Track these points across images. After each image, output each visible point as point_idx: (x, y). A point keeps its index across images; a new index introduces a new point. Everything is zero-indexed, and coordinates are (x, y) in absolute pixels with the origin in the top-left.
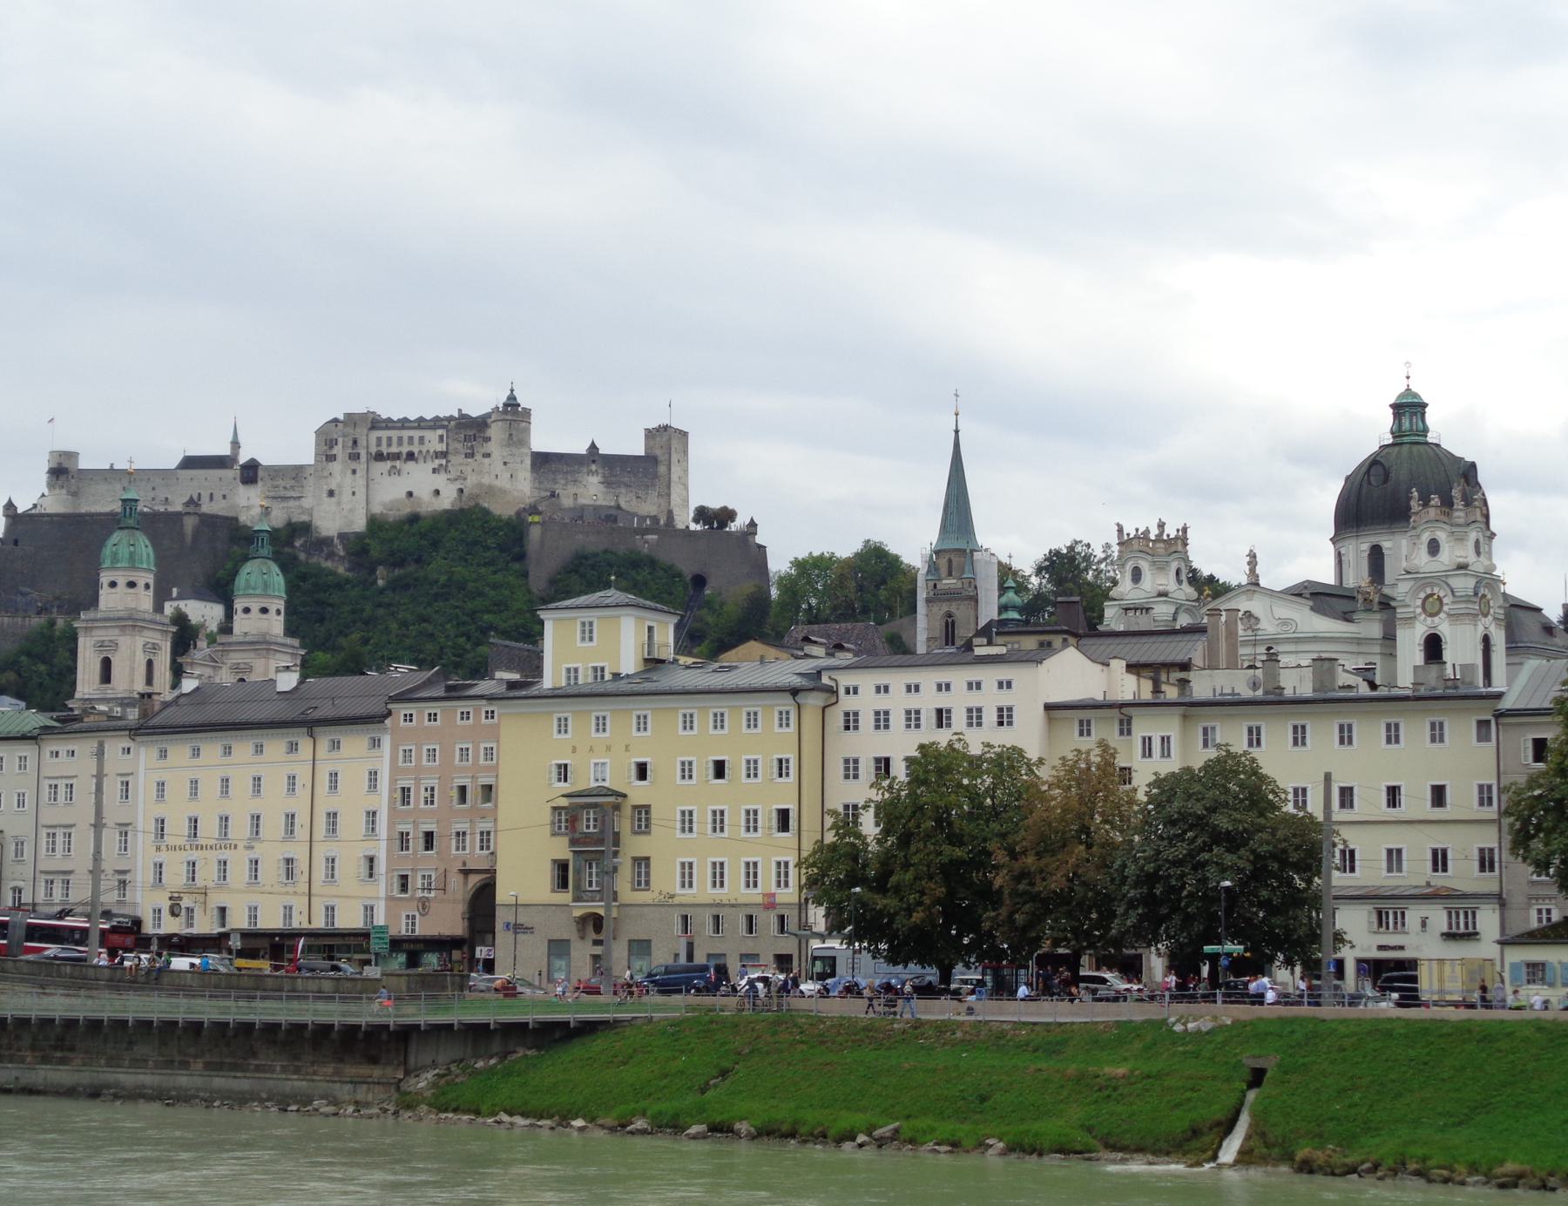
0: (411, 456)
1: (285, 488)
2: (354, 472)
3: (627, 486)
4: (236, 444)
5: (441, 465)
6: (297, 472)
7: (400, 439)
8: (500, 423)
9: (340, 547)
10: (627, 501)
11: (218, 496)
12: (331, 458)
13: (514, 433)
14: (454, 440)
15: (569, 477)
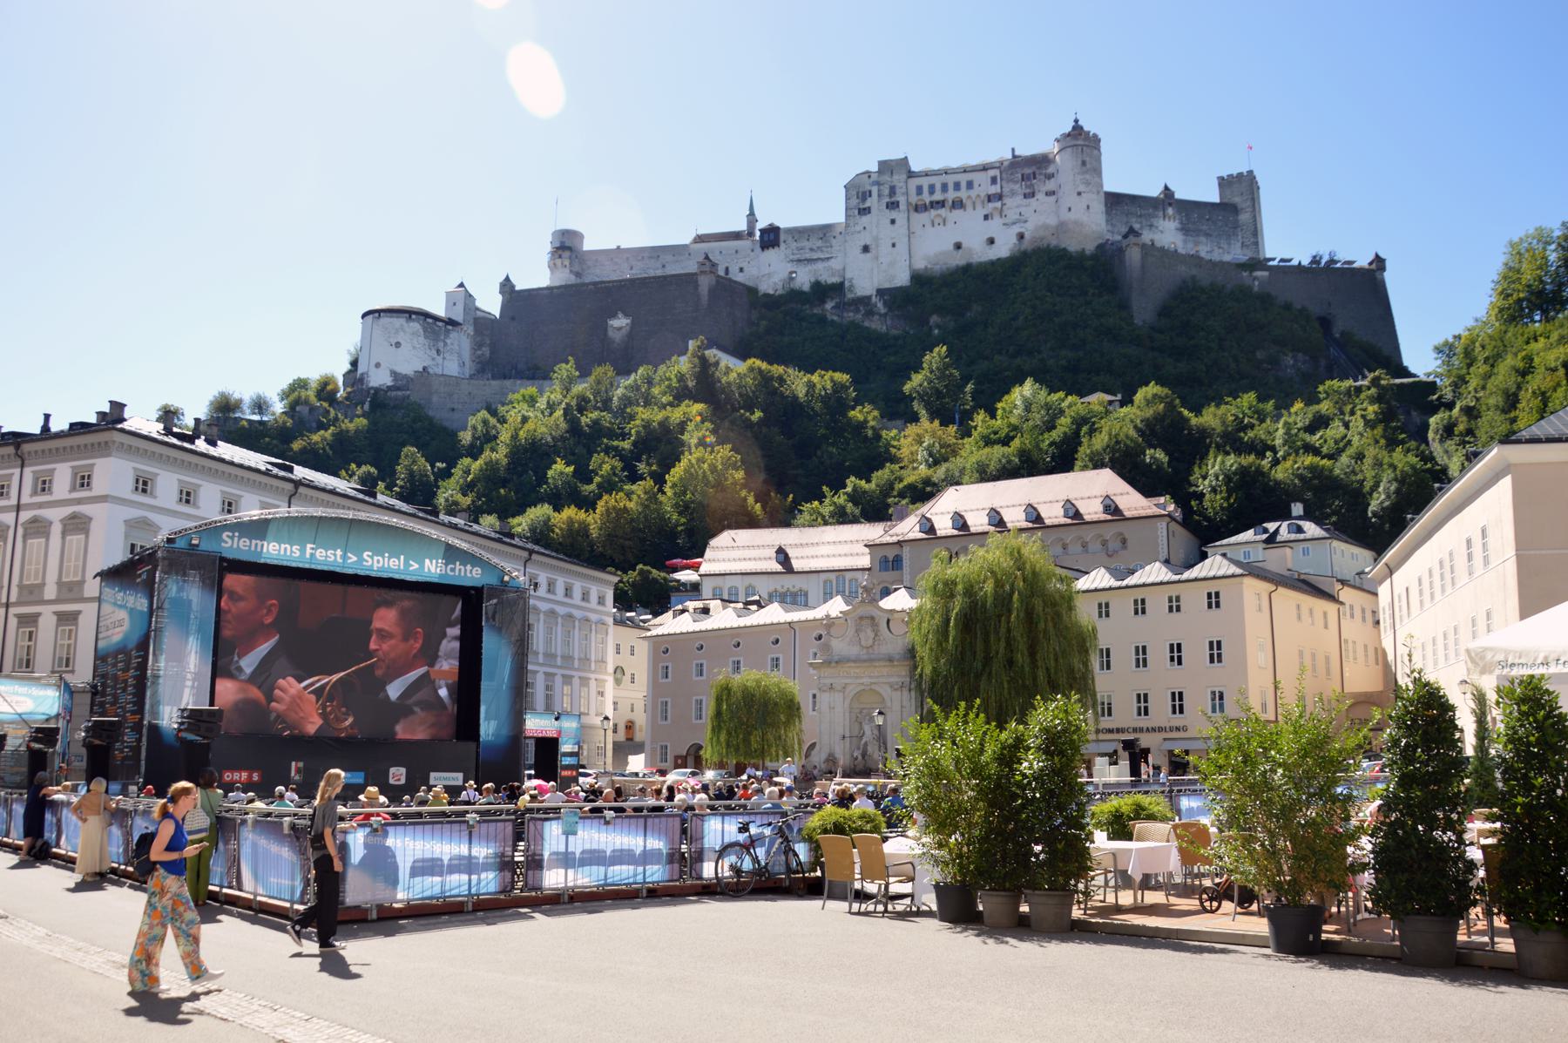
0: (958, 204)
1: (811, 250)
2: (893, 222)
3: (1207, 235)
4: (752, 214)
5: (996, 208)
6: (824, 231)
7: (945, 187)
8: (1069, 150)
9: (880, 305)
10: (1206, 250)
11: (734, 270)
12: (865, 211)
13: (1087, 159)
14: (1009, 181)
15: (1144, 224)
